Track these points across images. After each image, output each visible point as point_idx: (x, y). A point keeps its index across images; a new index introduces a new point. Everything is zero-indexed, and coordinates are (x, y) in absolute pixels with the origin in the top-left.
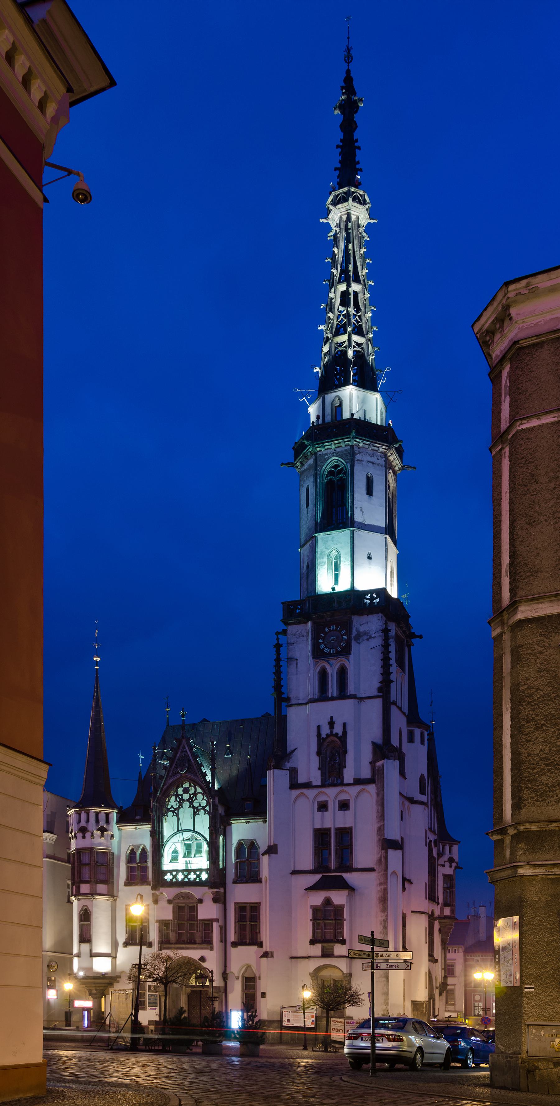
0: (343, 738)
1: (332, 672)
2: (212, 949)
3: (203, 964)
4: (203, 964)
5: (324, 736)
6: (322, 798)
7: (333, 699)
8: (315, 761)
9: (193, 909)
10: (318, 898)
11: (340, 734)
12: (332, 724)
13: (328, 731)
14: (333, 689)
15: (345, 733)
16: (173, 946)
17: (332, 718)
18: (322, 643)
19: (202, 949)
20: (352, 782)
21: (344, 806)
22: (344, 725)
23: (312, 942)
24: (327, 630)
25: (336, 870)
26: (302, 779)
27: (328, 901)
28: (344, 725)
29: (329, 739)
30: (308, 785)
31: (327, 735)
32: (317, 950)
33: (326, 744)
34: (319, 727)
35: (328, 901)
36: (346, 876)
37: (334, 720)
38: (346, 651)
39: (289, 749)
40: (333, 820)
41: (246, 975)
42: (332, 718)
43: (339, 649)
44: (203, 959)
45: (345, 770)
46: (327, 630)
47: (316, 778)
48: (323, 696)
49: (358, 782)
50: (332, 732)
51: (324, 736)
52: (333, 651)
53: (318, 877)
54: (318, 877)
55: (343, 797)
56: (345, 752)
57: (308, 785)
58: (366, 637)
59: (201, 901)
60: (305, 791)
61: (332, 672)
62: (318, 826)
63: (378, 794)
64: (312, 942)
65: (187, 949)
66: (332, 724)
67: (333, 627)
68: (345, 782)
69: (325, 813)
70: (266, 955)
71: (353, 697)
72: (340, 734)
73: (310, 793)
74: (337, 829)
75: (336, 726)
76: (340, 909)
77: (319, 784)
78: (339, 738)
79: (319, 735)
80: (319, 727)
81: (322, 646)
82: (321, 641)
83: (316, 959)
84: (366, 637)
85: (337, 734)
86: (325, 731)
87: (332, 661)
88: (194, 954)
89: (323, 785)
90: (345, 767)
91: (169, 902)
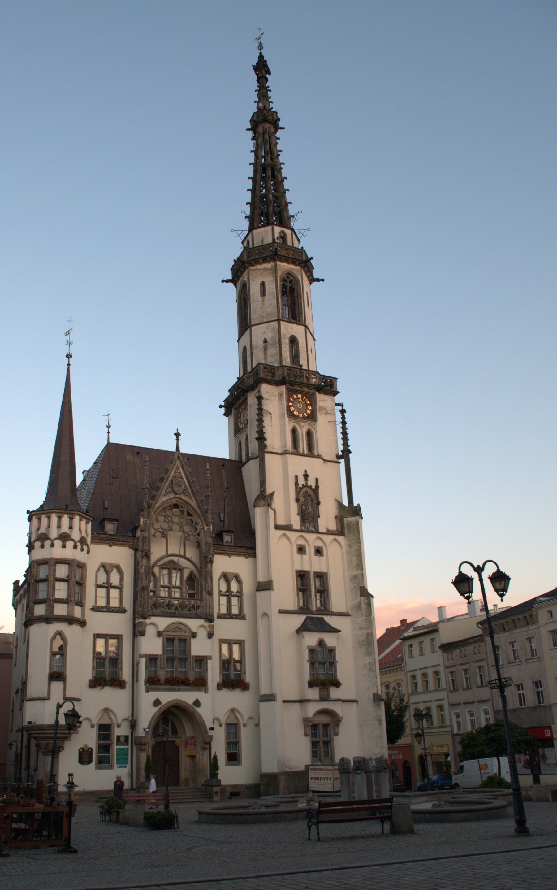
0: (316, 490)
2: (206, 692)
3: (197, 709)
4: (197, 709)
5: (300, 485)
6: (302, 542)
7: (303, 455)
8: (294, 508)
9: (185, 642)
10: (311, 639)
11: (314, 487)
12: (306, 476)
13: (304, 483)
14: (303, 446)
15: (317, 487)
16: (163, 687)
17: (306, 471)
18: (292, 406)
20: (325, 531)
21: (319, 551)
22: (317, 480)
23: (311, 684)
24: (295, 397)
25: (319, 611)
26: (281, 521)
27: (321, 643)
28: (317, 480)
29: (304, 490)
30: (288, 528)
31: (303, 485)
32: (314, 693)
33: (301, 493)
34: (296, 477)
35: (321, 643)
36: (328, 619)
37: (308, 473)
38: (312, 417)
39: (268, 491)
42: (306, 471)
43: (306, 415)
44: (197, 703)
45: (319, 520)
46: (295, 397)
47: (296, 522)
48: (296, 451)
49: (329, 532)
50: (307, 484)
51: (300, 485)
52: (301, 415)
53: (302, 618)
54: (303, 618)
55: (319, 544)
56: (318, 503)
57: (288, 528)
58: (324, 412)
59: (194, 635)
60: (288, 533)
62: (299, 568)
63: (350, 546)
65: (179, 690)
66: (306, 476)
67: (300, 396)
68: (320, 530)
69: (304, 556)
70: (270, 698)
71: (319, 457)
72: (314, 487)
73: (293, 536)
74: (315, 573)
75: (309, 478)
76: (332, 651)
77: (299, 528)
78: (313, 490)
79: (296, 484)
80: (296, 477)
81: (292, 409)
82: (291, 404)
83: (315, 703)
84: (324, 412)
85: (310, 487)
86: (301, 482)
87: (302, 424)
88: (187, 697)
89: (301, 531)
90: (319, 517)
91: (159, 634)
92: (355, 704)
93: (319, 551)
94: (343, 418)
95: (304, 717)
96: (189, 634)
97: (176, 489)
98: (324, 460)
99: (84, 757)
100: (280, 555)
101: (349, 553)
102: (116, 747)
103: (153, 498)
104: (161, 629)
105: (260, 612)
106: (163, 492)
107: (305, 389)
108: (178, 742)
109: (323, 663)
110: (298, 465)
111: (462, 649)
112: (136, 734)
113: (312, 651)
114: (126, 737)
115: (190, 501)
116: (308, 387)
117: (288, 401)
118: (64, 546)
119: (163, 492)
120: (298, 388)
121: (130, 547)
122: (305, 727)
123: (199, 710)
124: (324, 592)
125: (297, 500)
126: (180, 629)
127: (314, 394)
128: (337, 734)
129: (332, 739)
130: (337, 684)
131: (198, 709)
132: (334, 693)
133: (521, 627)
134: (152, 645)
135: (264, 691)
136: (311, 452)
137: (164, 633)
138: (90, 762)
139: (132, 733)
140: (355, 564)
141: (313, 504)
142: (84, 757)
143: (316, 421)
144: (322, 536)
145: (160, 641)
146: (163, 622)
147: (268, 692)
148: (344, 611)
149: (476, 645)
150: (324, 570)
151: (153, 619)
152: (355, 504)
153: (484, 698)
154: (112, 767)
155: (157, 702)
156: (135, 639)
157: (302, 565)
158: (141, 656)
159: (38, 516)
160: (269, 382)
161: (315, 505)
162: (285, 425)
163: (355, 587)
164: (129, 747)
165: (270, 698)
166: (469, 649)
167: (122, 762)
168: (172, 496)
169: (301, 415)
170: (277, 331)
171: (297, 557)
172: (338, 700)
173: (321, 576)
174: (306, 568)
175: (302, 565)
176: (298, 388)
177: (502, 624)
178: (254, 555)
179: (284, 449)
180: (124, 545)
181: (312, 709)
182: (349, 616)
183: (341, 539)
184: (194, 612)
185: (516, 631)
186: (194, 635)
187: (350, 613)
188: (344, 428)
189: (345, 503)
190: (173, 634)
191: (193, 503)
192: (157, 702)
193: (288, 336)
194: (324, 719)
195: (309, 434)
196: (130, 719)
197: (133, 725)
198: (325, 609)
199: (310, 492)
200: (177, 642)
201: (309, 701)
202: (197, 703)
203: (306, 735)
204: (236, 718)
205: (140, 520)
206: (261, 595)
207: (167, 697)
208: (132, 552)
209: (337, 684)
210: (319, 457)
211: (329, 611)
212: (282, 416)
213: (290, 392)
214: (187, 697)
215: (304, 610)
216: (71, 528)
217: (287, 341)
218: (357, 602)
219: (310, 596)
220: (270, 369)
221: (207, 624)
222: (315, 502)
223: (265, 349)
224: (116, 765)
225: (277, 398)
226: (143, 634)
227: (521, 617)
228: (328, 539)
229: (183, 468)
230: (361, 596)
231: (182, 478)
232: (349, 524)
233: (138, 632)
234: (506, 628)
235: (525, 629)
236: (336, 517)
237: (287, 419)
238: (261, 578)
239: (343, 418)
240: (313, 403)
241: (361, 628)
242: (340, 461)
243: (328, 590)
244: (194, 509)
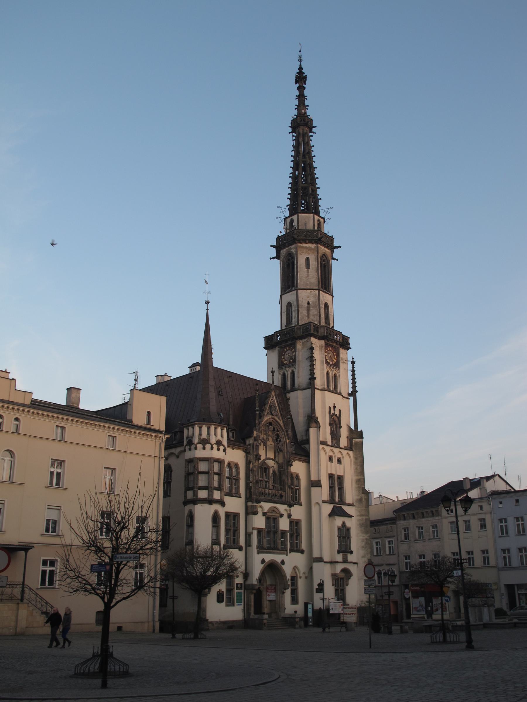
0: (339, 418)
1: (331, 375)
3: (282, 566)
4: (282, 566)
6: (331, 454)
10: (339, 521)
12: (334, 407)
16: (265, 551)
19: (281, 554)
20: (343, 447)
21: (339, 461)
22: (340, 410)
23: (339, 552)
27: (344, 523)
28: (340, 410)
30: (324, 443)
32: (339, 558)
34: (330, 407)
35: (344, 523)
36: (345, 508)
40: (337, 470)
41: (293, 575)
44: (283, 562)
49: (345, 448)
55: (340, 456)
56: (340, 427)
57: (324, 443)
59: (282, 515)
61: (331, 375)
63: (356, 458)
64: (339, 552)
65: (273, 553)
66: (334, 407)
68: (342, 446)
70: (320, 560)
71: (340, 394)
73: (328, 449)
74: (338, 476)
75: (336, 409)
76: (348, 529)
79: (330, 412)
80: (330, 407)
88: (277, 558)
92: (356, 565)
93: (339, 461)
94: (353, 367)
95: (333, 573)
96: (278, 515)
97: (273, 412)
98: (343, 397)
99: (220, 598)
100: (324, 462)
101: (355, 463)
102: (236, 591)
103: (261, 417)
104: (266, 511)
105: (313, 502)
106: (266, 414)
107: (334, 344)
108: (262, 588)
109: (344, 538)
110: (331, 399)
111: (376, 528)
112: (248, 582)
113: (339, 529)
114: (241, 584)
115: (279, 421)
116: (336, 343)
117: (325, 352)
118: (218, 450)
119: (266, 414)
120: (331, 343)
121: (243, 451)
122: (333, 580)
123: (283, 566)
124: (341, 488)
125: (330, 424)
126: (274, 511)
127: (339, 348)
128: (347, 585)
129: (345, 588)
130: (352, 552)
131: (283, 566)
132: (350, 558)
133: (427, 517)
134: (259, 521)
135: (316, 554)
136: (336, 391)
137: (268, 514)
138: (223, 601)
139: (245, 582)
140: (359, 471)
141: (336, 427)
142: (220, 598)
143: (339, 368)
144: (342, 451)
145: (263, 518)
146: (266, 506)
147: (319, 556)
148: (351, 503)
149: (389, 526)
150: (342, 474)
151: (262, 504)
152: (359, 430)
153: (392, 562)
154: (233, 605)
155: (263, 561)
156: (247, 516)
157: (331, 470)
158: (253, 529)
159: (200, 425)
160: (315, 337)
161: (338, 428)
162: (323, 370)
163: (359, 487)
164: (243, 591)
165: (320, 560)
166: (383, 528)
167: (239, 601)
168: (270, 416)
169: (331, 363)
170: (317, 298)
171: (329, 463)
172: (352, 563)
173: (340, 478)
174: (333, 472)
175: (331, 470)
176: (331, 343)
177: (413, 514)
178: (308, 462)
179: (323, 387)
180: (240, 449)
181: (339, 568)
182: (354, 506)
183: (351, 453)
184: (280, 500)
185: (423, 519)
186: (282, 515)
187: (354, 504)
188: (353, 375)
189: (353, 427)
190: (271, 514)
191: (281, 423)
192: (263, 561)
193: (324, 303)
194: (342, 575)
195: (335, 376)
196: (244, 572)
197: (246, 575)
198: (342, 501)
199: (336, 419)
200: (272, 519)
201: (338, 562)
202: (283, 562)
203: (333, 585)
204: (296, 573)
205: (253, 432)
206: (314, 490)
207: (268, 557)
208: (244, 454)
209: (352, 552)
210: (340, 394)
211: (343, 502)
212: (322, 362)
213: (327, 345)
214: (277, 558)
215: (332, 501)
216: (222, 436)
217: (323, 306)
218: (359, 497)
219: (335, 491)
220: (317, 328)
221: (288, 508)
222: (338, 426)
223: (308, 310)
224: (236, 604)
225: (318, 349)
226: (255, 513)
227: (429, 511)
228: (345, 452)
229: (276, 398)
230: (363, 493)
231: (275, 404)
232: (356, 443)
233: (250, 512)
234: (416, 517)
235: (431, 519)
236: (347, 437)
237: (325, 365)
238: (313, 478)
239: (353, 367)
240: (338, 355)
241: (361, 515)
242: (350, 397)
243: (343, 488)
244: (281, 427)
